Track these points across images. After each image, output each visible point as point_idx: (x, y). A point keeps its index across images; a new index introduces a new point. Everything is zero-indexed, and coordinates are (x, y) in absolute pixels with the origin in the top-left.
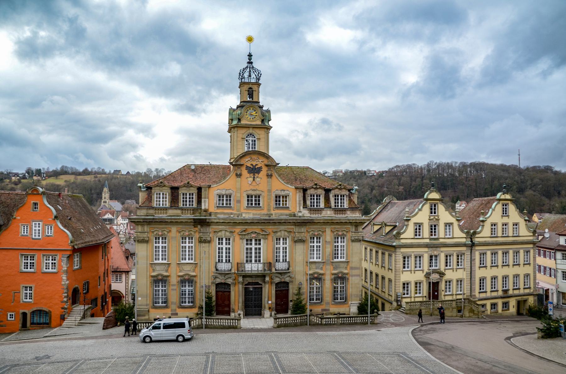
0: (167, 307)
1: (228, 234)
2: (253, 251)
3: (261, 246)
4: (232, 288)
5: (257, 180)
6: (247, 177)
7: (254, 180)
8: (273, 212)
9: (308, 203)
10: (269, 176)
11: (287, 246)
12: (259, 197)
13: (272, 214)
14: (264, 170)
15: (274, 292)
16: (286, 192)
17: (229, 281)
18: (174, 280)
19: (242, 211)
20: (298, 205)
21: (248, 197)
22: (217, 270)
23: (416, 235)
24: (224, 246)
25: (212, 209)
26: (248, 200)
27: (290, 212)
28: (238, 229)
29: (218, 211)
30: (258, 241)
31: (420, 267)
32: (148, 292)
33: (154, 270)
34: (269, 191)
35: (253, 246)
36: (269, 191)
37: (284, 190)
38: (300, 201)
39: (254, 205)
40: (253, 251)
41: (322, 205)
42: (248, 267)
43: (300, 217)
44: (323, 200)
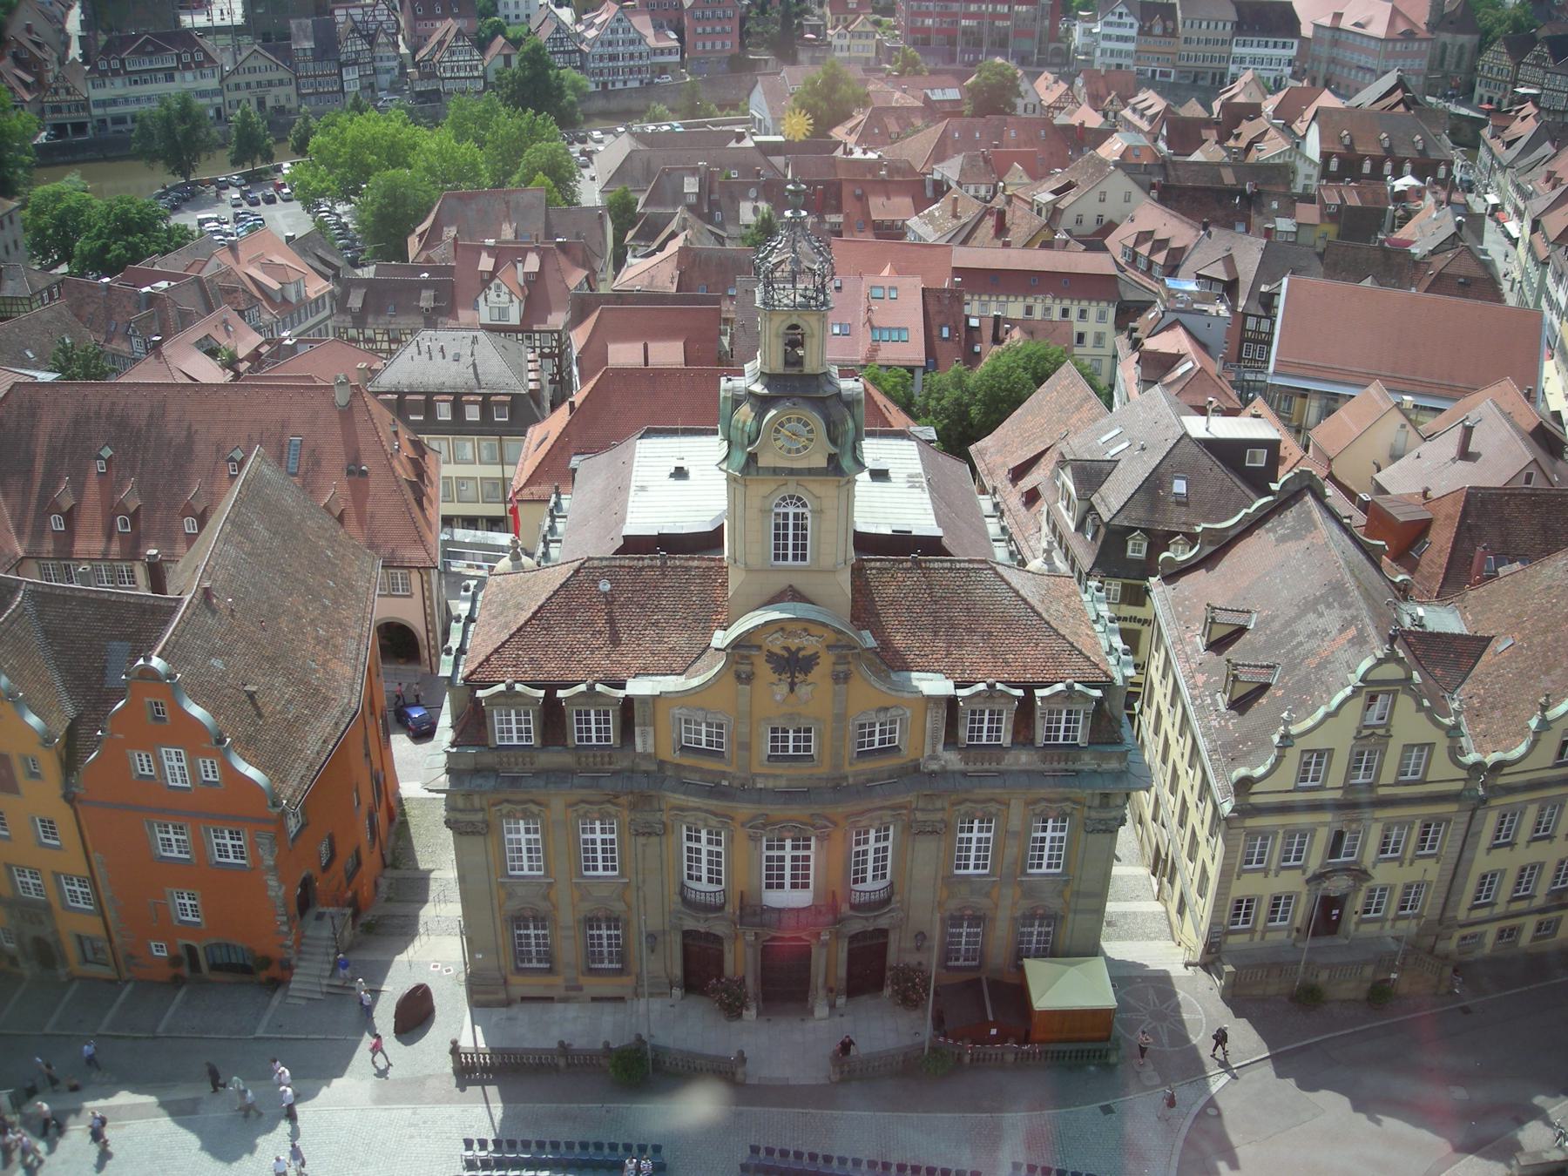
0: (550, 971)
1: (713, 821)
2: (788, 863)
3: (811, 853)
4: (726, 948)
5: (803, 691)
6: (771, 691)
7: (792, 690)
8: (847, 769)
9: (963, 733)
10: (841, 678)
11: (889, 844)
12: (808, 730)
13: (846, 778)
14: (826, 662)
15: (843, 956)
16: (893, 712)
17: (719, 929)
18: (567, 916)
19: (756, 769)
20: (928, 740)
21: (774, 730)
22: (686, 901)
23: (1305, 780)
24: (704, 846)
25: (669, 754)
26: (774, 739)
27: (902, 761)
28: (744, 810)
29: (688, 761)
30: (801, 842)
31: (1298, 859)
32: (500, 941)
33: (510, 896)
34: (841, 718)
35: (788, 853)
36: (841, 718)
37: (886, 709)
38: (935, 730)
39: (791, 752)
40: (788, 863)
41: (1006, 739)
42: (773, 898)
43: (932, 774)
44: (1010, 727)
